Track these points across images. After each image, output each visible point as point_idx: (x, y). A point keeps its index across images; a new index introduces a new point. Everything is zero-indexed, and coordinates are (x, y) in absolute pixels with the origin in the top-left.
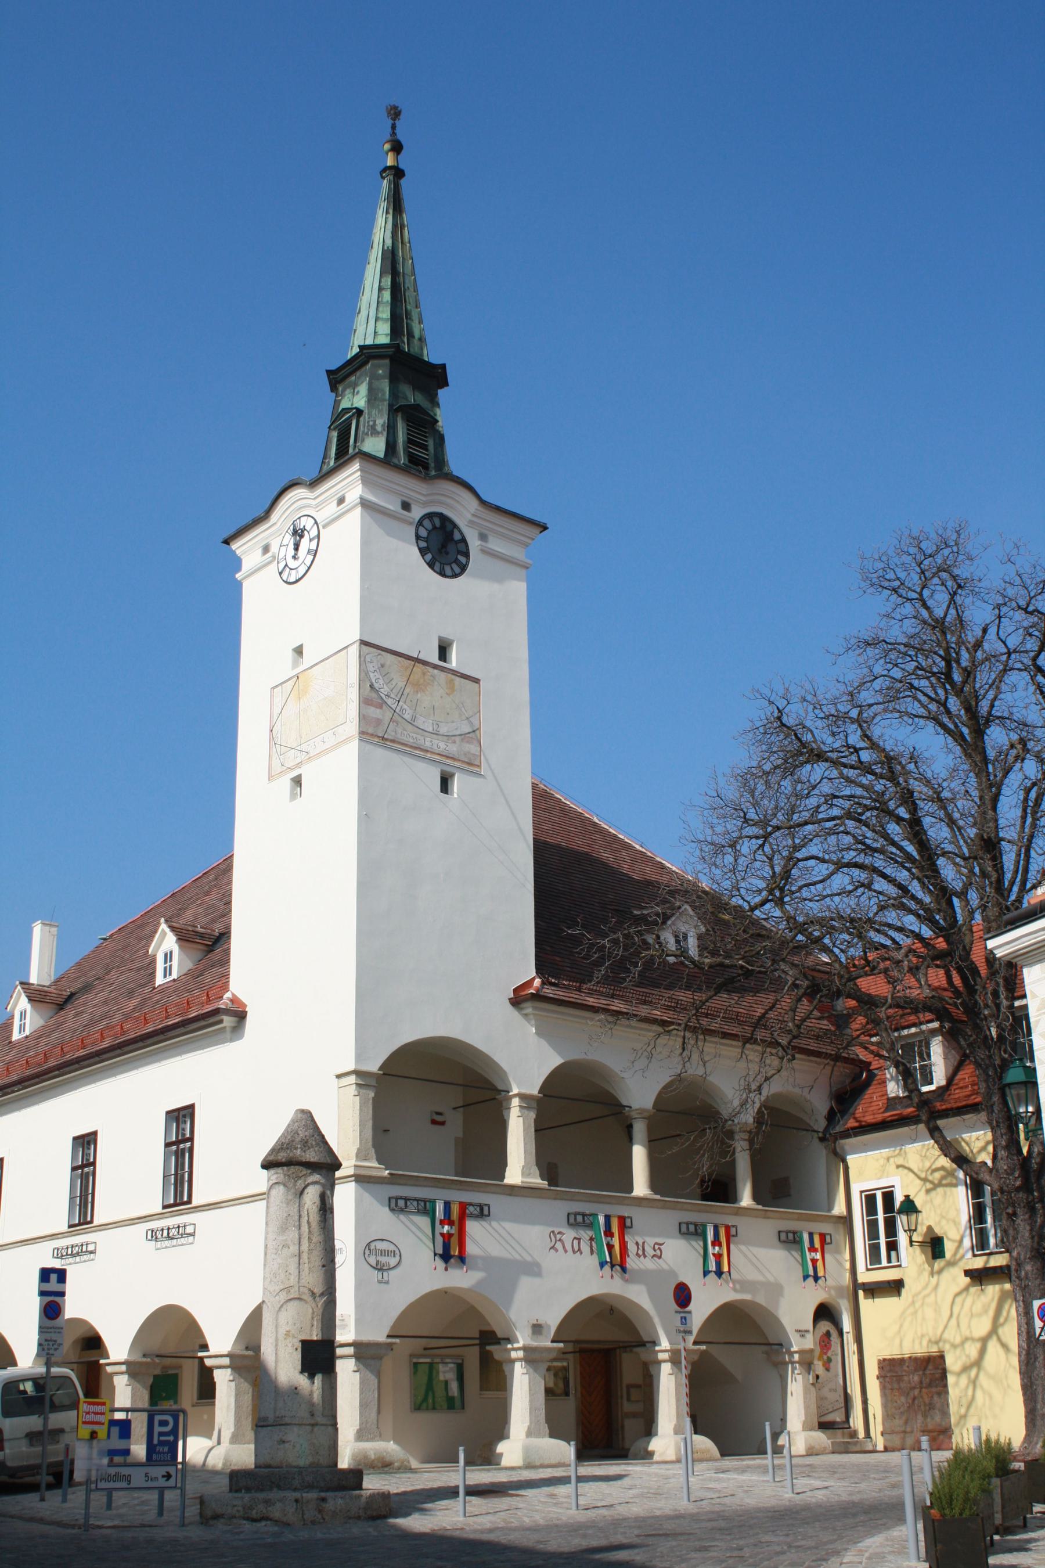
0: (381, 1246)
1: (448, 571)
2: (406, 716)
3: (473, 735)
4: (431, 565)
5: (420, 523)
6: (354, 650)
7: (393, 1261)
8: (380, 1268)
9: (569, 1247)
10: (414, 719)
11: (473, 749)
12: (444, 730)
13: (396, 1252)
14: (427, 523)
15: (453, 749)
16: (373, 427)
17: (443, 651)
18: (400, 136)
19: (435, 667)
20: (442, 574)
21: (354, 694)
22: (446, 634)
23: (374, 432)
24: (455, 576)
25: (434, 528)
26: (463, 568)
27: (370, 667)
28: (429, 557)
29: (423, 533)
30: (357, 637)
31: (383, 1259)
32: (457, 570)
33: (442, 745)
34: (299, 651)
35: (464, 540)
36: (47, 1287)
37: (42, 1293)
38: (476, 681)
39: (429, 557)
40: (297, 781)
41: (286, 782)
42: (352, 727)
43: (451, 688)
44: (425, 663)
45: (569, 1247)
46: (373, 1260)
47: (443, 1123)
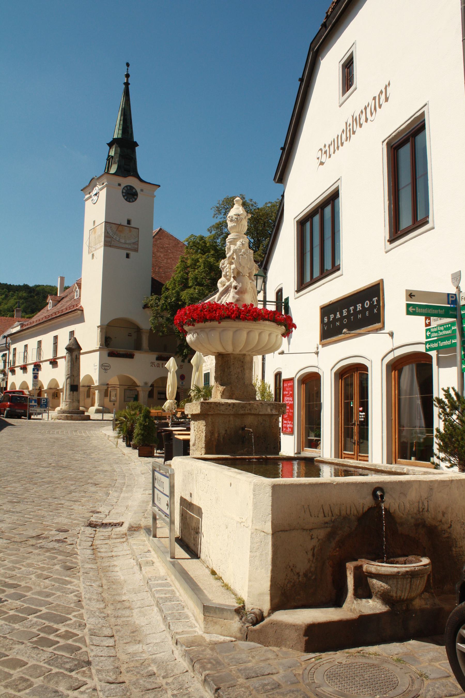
0: (105, 365)
1: (131, 200)
2: (118, 240)
3: (137, 243)
4: (126, 200)
5: (124, 189)
6: (104, 224)
7: (108, 368)
8: (105, 370)
9: (156, 365)
10: (119, 240)
11: (136, 246)
12: (127, 242)
13: (109, 366)
14: (126, 189)
15: (130, 247)
16: (115, 161)
17: (129, 222)
18: (129, 73)
19: (126, 226)
20: (129, 202)
21: (103, 235)
22: (130, 218)
23: (115, 163)
24: (133, 201)
25: (128, 189)
26: (136, 199)
27: (108, 228)
28: (126, 197)
29: (124, 191)
30: (104, 220)
31: (106, 368)
32: (134, 200)
33: (127, 246)
34: (94, 222)
35: (136, 191)
36: (35, 372)
37: (33, 373)
38: (138, 229)
39: (126, 197)
40: (93, 255)
41: (91, 255)
42: (102, 243)
43: (130, 231)
44: (123, 225)
45: (156, 365)
46: (103, 368)
47: (131, 336)
